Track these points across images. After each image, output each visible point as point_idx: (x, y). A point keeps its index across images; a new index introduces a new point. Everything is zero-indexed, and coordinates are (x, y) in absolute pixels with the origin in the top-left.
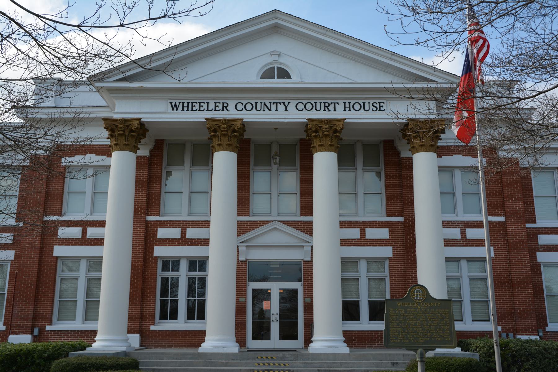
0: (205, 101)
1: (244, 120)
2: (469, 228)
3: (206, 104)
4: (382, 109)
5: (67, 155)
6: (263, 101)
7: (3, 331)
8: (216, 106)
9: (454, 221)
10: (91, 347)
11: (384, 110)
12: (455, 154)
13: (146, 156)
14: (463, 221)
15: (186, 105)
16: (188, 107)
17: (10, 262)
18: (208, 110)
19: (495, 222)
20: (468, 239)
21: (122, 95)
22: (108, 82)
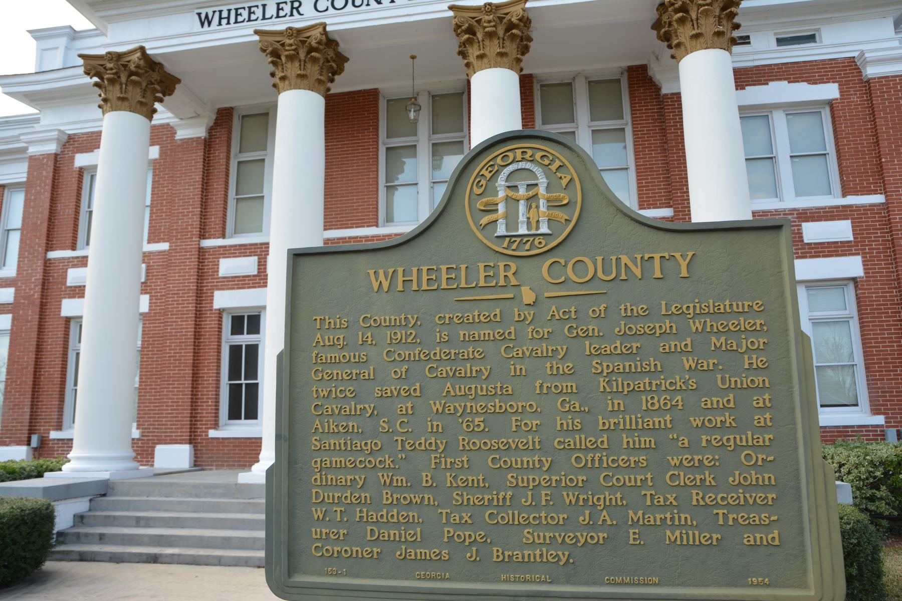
2: (808, 221)
3: (261, 8)
8: (278, 9)
9: (776, 211)
10: (60, 470)
12: (773, 80)
13: (200, 138)
14: (794, 210)
15: (225, 14)
16: (228, 18)
18: (264, 18)
19: (863, 206)
20: (808, 244)
21: (115, 12)
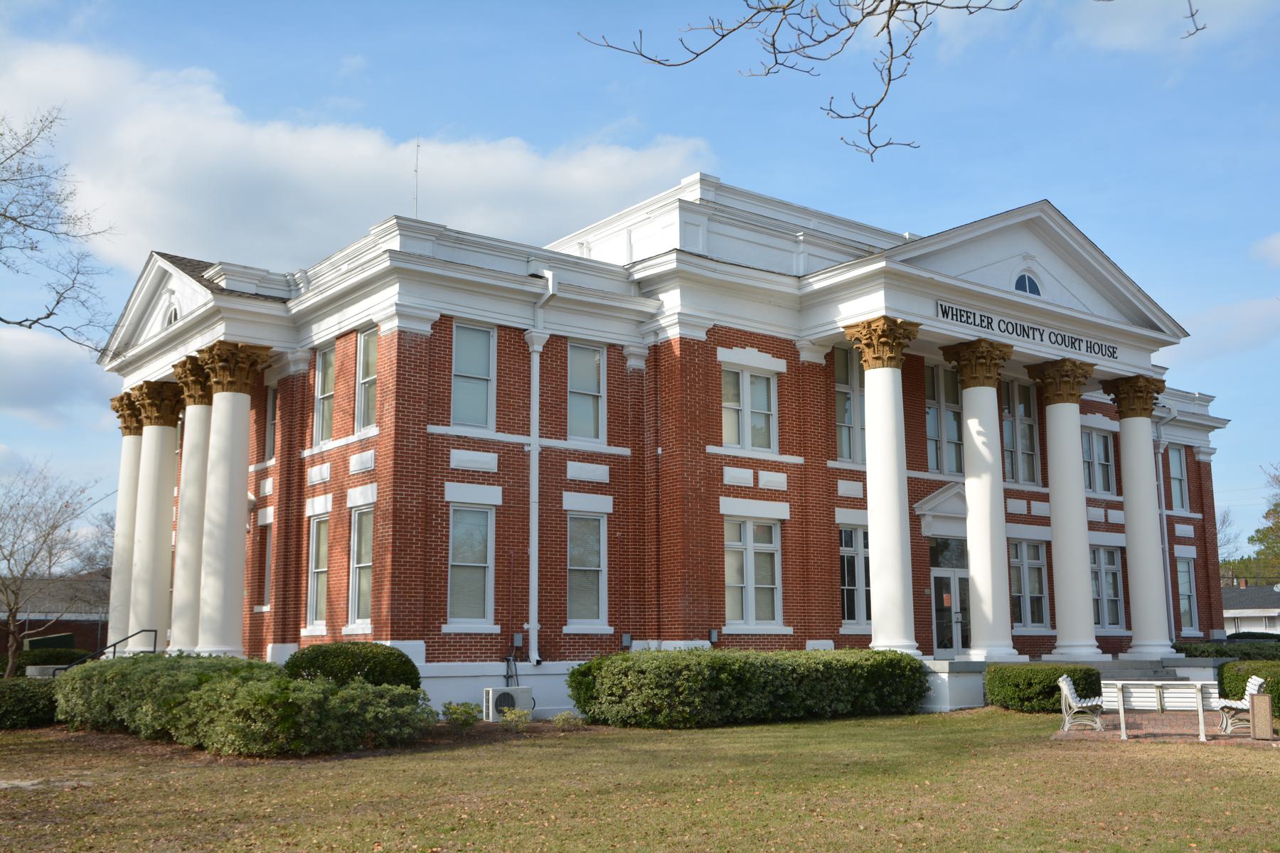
0: (972, 311)
1: (1015, 348)
4: (1115, 356)
5: (729, 346)
6: (1022, 323)
7: (611, 635)
15: (955, 313)
16: (957, 315)
17: (606, 516)
22: (894, 262)
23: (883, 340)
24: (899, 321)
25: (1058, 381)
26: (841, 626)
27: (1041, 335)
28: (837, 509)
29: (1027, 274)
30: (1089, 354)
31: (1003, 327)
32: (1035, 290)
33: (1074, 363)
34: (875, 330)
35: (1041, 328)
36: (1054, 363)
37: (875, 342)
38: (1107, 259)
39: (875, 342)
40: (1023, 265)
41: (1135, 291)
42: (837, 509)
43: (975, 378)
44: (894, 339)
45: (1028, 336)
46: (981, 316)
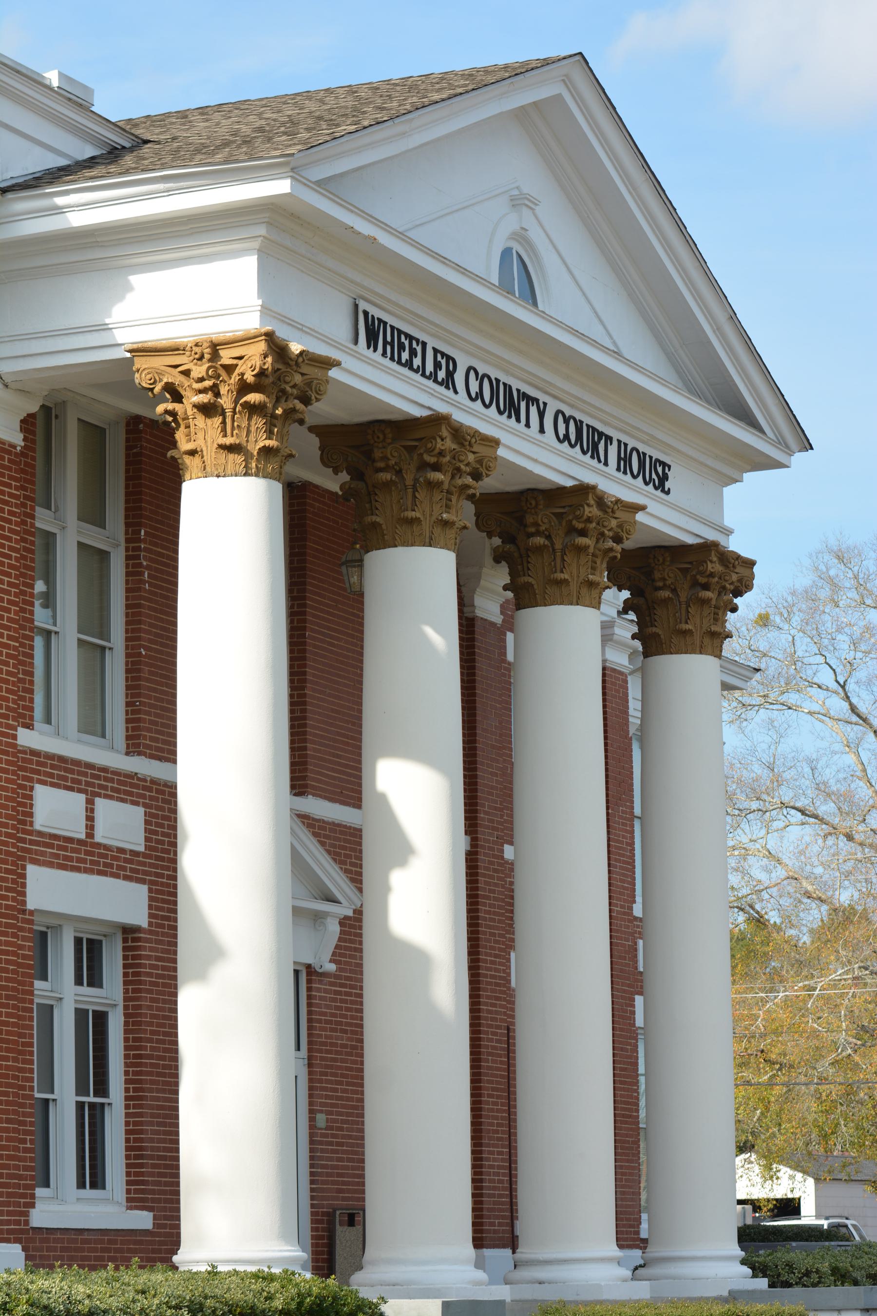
0: (422, 337)
4: (667, 485)
11: (668, 493)
13: (15, 447)
23: (254, 398)
24: (295, 348)
25: (558, 546)
26: (33, 1205)
27: (541, 415)
28: (32, 870)
29: (516, 247)
30: (620, 475)
31: (474, 387)
32: (531, 297)
33: (601, 500)
34: (229, 369)
35: (542, 398)
36: (559, 492)
37: (226, 401)
38: (680, 226)
39: (226, 401)
40: (511, 224)
41: (722, 317)
42: (32, 870)
43: (412, 522)
44: (278, 400)
45: (518, 420)
46: (436, 351)
